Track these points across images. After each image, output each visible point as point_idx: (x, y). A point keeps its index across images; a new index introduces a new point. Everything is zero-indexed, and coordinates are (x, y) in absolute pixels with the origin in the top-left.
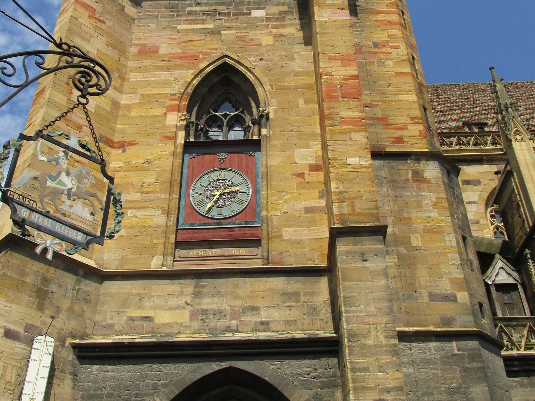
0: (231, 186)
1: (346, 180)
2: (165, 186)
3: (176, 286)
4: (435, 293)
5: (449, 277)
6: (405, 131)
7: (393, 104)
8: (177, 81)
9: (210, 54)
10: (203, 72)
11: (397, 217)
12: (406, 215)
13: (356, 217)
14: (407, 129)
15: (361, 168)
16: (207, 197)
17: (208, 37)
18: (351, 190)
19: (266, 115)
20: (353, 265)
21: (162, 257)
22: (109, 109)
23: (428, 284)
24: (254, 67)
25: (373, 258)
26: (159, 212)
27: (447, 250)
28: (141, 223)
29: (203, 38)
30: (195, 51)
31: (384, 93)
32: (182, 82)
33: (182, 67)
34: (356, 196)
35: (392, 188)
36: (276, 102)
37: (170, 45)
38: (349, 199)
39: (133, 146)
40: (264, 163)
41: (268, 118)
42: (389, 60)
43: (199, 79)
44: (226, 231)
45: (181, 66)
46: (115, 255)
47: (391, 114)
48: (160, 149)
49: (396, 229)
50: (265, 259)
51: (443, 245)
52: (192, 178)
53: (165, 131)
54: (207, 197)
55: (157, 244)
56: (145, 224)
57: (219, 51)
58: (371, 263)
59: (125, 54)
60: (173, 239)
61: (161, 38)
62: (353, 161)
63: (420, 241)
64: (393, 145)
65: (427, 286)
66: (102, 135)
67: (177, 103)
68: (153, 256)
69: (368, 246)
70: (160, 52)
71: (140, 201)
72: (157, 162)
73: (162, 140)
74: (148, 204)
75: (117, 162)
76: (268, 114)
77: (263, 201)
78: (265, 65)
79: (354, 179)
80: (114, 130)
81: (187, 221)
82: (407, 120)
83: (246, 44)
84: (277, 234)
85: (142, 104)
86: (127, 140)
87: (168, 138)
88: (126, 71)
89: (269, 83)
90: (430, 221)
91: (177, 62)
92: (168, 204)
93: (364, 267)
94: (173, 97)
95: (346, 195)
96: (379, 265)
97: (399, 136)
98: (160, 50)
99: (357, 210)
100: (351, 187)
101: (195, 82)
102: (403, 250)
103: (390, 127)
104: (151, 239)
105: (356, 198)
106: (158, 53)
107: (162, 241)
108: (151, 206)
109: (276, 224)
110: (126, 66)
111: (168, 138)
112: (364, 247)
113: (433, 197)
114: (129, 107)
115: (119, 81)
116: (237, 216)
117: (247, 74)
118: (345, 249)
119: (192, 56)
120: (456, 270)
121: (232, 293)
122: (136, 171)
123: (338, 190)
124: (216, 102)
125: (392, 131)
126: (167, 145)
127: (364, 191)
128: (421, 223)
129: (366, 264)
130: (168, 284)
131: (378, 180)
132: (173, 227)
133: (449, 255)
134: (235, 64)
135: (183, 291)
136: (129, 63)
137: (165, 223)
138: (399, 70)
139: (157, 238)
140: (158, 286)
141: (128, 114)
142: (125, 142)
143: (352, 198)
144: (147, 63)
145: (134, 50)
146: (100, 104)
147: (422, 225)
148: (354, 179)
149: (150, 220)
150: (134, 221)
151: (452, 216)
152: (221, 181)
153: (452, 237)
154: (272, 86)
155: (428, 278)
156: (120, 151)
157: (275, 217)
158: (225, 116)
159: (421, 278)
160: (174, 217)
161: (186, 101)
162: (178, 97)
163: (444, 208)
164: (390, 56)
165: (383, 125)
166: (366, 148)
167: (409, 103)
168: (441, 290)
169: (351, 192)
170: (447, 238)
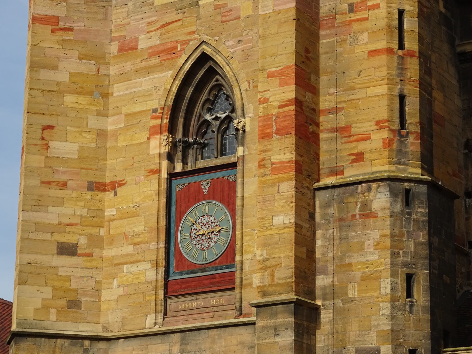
0: (215, 223)
1: (270, 245)
2: (153, 234)
3: (166, 345)
4: (361, 348)
5: (377, 330)
6: (368, 141)
7: (360, 102)
8: (157, 89)
9: (186, 42)
10: (182, 72)
11: (338, 264)
12: (347, 261)
13: (274, 288)
14: (369, 138)
15: (285, 228)
16: (193, 239)
17: (185, 14)
18: (273, 256)
19: (242, 128)
20: (267, 341)
21: (154, 315)
22: (94, 145)
23: (357, 339)
24: (231, 56)
25: (283, 332)
26: (149, 266)
27: (380, 299)
28: (135, 280)
29: (180, 16)
30: (173, 40)
31: (352, 89)
32: (162, 89)
33: (160, 67)
34: (276, 263)
35: (338, 229)
36: (252, 107)
37: (148, 34)
38: (270, 267)
39: (123, 187)
40: (239, 194)
41: (244, 131)
42: (364, 32)
43: (178, 83)
44: (209, 279)
45: (160, 66)
46: (118, 316)
47: (356, 119)
48: (146, 187)
49: (335, 279)
50: (237, 311)
51: (376, 293)
52: (180, 216)
53: (148, 163)
54: (193, 239)
55: (149, 301)
56: (139, 281)
57: (197, 36)
58: (281, 338)
59: (104, 58)
60: (161, 294)
61: (139, 24)
62: (279, 220)
63: (356, 291)
64: (352, 166)
65: (356, 341)
66: (90, 182)
67: (158, 122)
68: (147, 315)
69: (282, 320)
70: (139, 47)
71: (133, 255)
72: (144, 205)
73: (147, 176)
74: (140, 258)
75: (111, 209)
76: (244, 126)
77: (238, 244)
78: (243, 51)
79: (277, 243)
80: (104, 169)
81: (178, 270)
82: (371, 126)
83: (224, 19)
84: (248, 281)
85: (127, 127)
86: (117, 179)
87: (153, 172)
88: (109, 82)
89: (246, 79)
90: (370, 266)
91: (156, 60)
92: (156, 256)
93: (275, 342)
94: (155, 114)
95: (268, 263)
96: (288, 339)
97: (359, 152)
98: (139, 43)
99: (277, 281)
100: (273, 253)
101: (175, 89)
102: (339, 302)
103: (352, 139)
104: (144, 297)
105: (276, 265)
106: (137, 49)
107: (154, 297)
108: (142, 259)
109: (247, 270)
110: (108, 76)
111: (153, 172)
112: (278, 321)
113: (376, 234)
114: (115, 134)
115: (101, 101)
116: (219, 259)
117: (225, 68)
118: (262, 324)
119: (170, 48)
120: (385, 321)
121: (210, 348)
122: (127, 218)
123: (262, 257)
124: (207, 100)
125: (353, 145)
126: (152, 181)
127: (284, 257)
128: (360, 269)
129: (278, 339)
130: (160, 344)
131: (326, 220)
132: (162, 282)
133: (381, 305)
134: (212, 55)
135: (171, 350)
136: (112, 68)
137: (155, 277)
138: (372, 47)
139: (149, 295)
140: (152, 346)
141: (115, 144)
142: (115, 182)
143: (273, 266)
144: (128, 66)
145: (114, 48)
146: (83, 145)
147: (361, 271)
148: (277, 243)
149: (142, 275)
150: (130, 277)
151: (394, 255)
152: (205, 216)
153: (388, 283)
154: (249, 83)
155: (358, 332)
156: (112, 194)
157: (247, 261)
158: (217, 118)
159: (351, 333)
160: (162, 269)
161: (167, 118)
162: (159, 113)
163: (385, 248)
164: (367, 25)
165: (345, 137)
166: (292, 203)
167: (377, 98)
168: (367, 344)
169: (273, 258)
170: (382, 285)
